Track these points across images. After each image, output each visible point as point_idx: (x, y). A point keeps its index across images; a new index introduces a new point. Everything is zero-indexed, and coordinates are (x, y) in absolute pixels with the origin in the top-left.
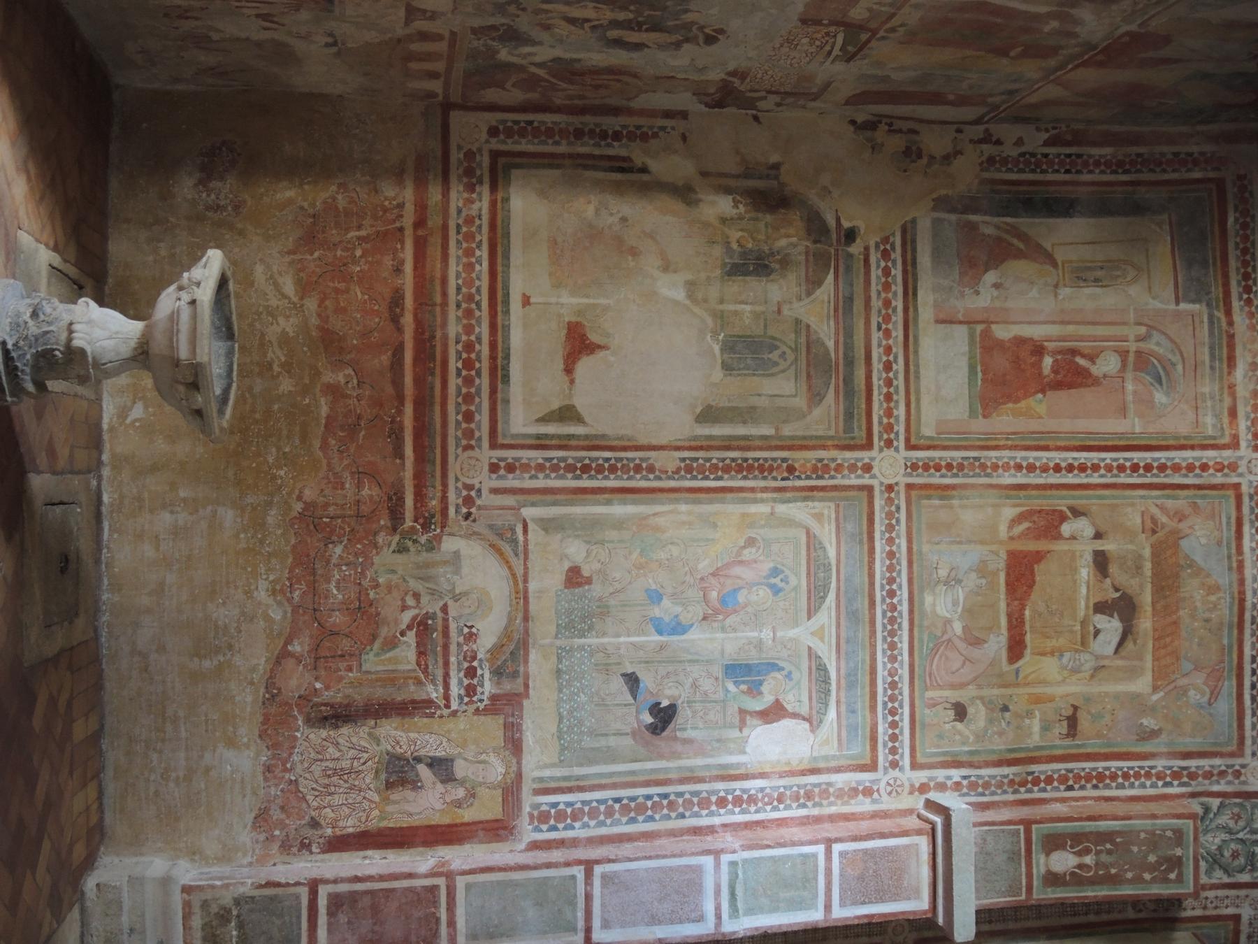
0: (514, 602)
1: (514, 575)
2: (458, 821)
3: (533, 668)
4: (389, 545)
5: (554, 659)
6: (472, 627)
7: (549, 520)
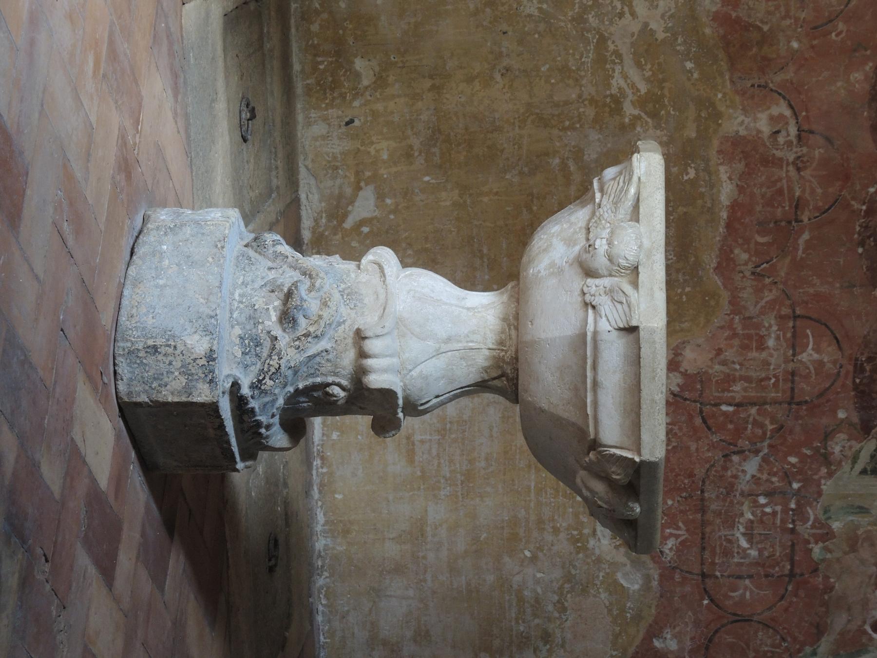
4: (855, 459)
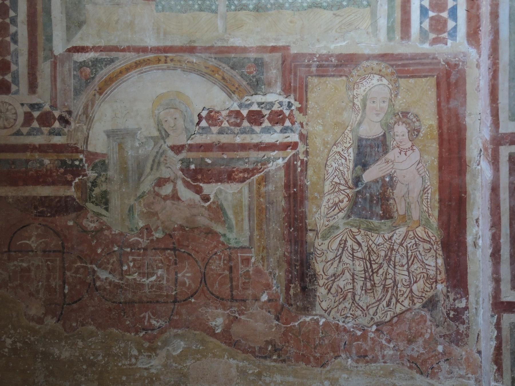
0: (171, 64)
1: (138, 64)
2: (436, 133)
3: (252, 41)
4: (98, 215)
5: (242, 14)
6: (199, 115)
7: (69, 17)
